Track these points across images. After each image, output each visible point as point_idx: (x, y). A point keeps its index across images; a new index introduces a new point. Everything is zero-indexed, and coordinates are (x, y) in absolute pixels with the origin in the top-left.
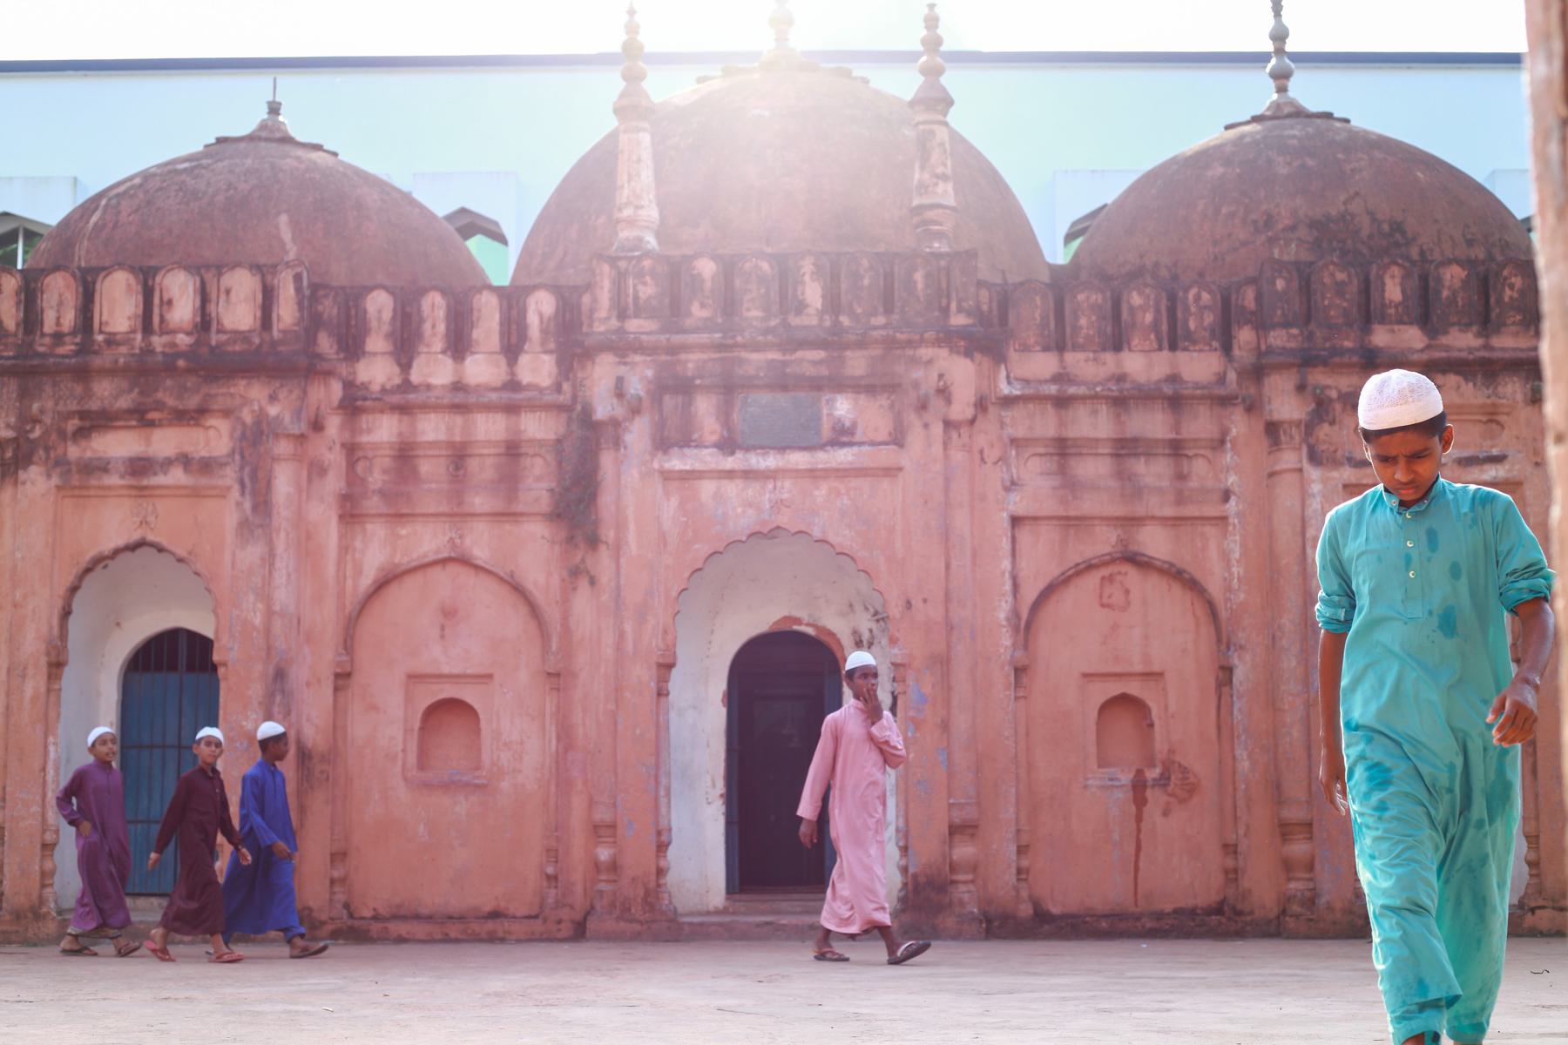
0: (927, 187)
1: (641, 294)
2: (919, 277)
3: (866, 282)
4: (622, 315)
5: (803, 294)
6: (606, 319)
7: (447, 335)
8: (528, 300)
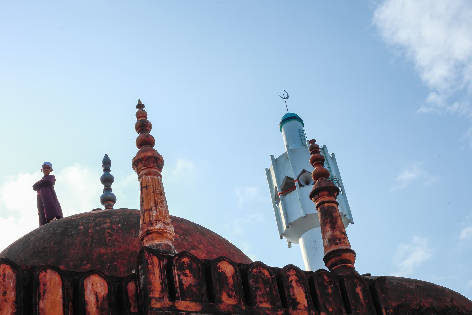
0: (340, 239)
1: (183, 283)
2: (359, 290)
3: (330, 291)
4: (173, 297)
5: (294, 295)
6: (159, 298)
7: (17, 302)
8: (85, 281)
